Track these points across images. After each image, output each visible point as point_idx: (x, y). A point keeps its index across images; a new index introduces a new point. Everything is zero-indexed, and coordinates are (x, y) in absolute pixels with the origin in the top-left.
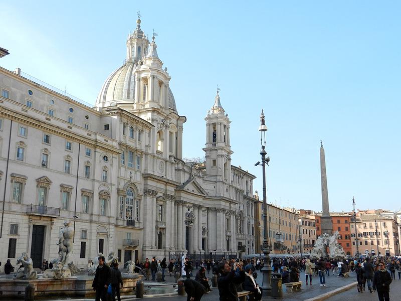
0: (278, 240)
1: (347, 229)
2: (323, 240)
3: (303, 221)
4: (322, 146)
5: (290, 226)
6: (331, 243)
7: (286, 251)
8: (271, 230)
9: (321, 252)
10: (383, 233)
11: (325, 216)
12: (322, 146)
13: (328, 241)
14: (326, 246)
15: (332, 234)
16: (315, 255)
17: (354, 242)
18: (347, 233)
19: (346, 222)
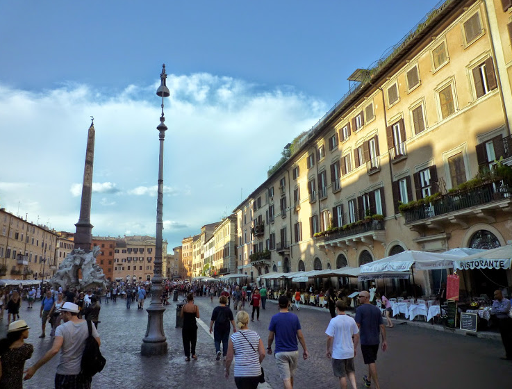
0: (20, 262)
1: (111, 254)
2: (75, 258)
3: (61, 244)
4: (92, 124)
5: (43, 246)
6: (86, 263)
7: (31, 276)
8: (9, 248)
9: (69, 277)
10: (146, 259)
11: (83, 223)
12: (92, 124)
13: (83, 260)
14: (78, 270)
15: (88, 251)
16: (57, 281)
17: (116, 268)
18: (111, 258)
19: (111, 246)
